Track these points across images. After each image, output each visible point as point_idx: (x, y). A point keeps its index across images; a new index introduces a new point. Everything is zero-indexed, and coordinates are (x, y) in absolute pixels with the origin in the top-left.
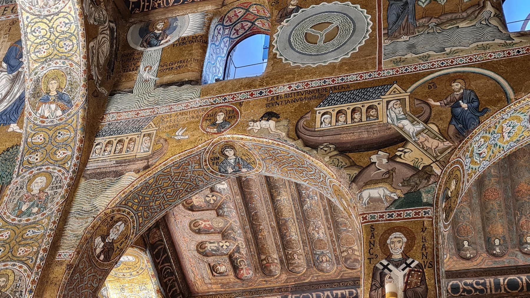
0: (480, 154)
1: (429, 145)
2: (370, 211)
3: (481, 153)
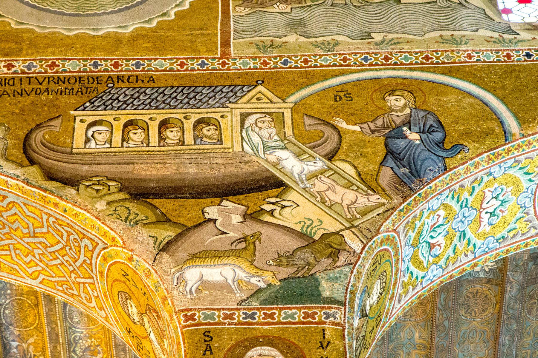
1: (337, 198)
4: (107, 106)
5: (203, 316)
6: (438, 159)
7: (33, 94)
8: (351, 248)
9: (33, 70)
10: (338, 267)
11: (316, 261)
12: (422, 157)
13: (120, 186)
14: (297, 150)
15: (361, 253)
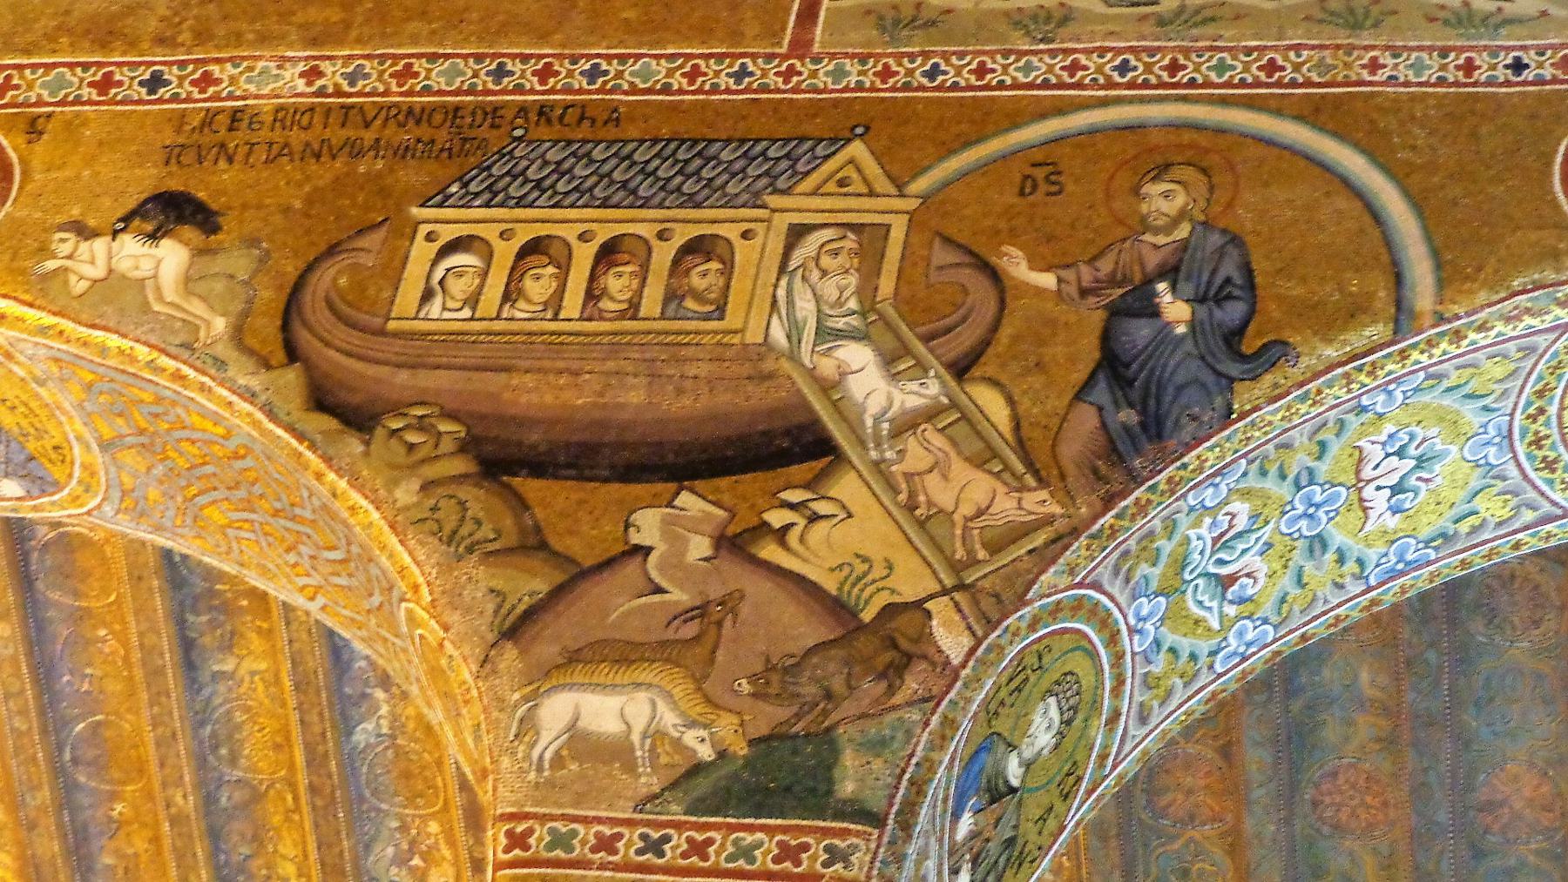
0: (1227, 582)
1: (945, 499)
2: (557, 804)
3: (1232, 579)
4: (496, 194)
5: (548, 839)
6: (1218, 384)
8: (940, 651)
10: (894, 708)
11: (850, 687)
12: (1180, 378)
13: (463, 434)
14: (889, 342)
15: (964, 665)
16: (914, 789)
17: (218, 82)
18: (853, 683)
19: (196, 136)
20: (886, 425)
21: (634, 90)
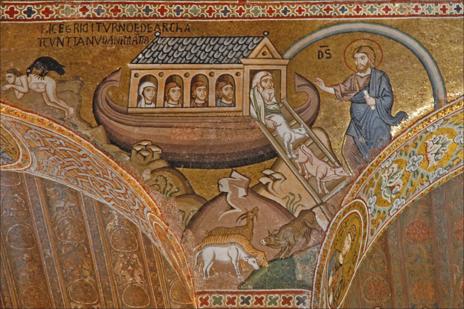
1: (313, 172)
4: (154, 58)
7: (101, 44)
8: (320, 227)
9: (101, 14)
10: (309, 247)
13: (160, 152)
14: (288, 115)
15: (327, 231)
16: (319, 275)
17: (51, 12)
18: (296, 239)
19: (48, 34)
20: (291, 145)
21: (193, 18)
